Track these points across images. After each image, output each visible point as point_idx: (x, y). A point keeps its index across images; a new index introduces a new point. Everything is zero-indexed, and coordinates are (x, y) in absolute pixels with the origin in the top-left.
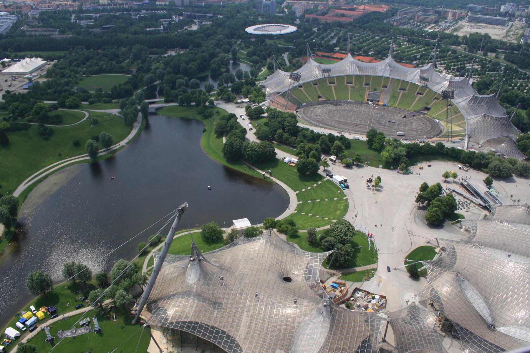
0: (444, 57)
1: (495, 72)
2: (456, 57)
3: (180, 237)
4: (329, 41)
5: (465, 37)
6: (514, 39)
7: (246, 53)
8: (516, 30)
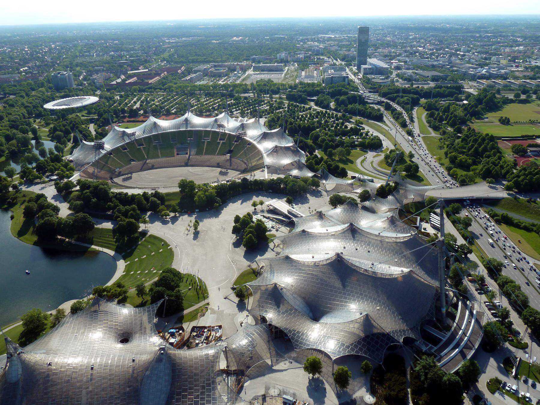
0: (238, 104)
1: (281, 110)
2: (248, 103)
3: (16, 327)
4: (132, 106)
5: (252, 84)
6: (292, 80)
7: (48, 130)
8: (291, 73)
